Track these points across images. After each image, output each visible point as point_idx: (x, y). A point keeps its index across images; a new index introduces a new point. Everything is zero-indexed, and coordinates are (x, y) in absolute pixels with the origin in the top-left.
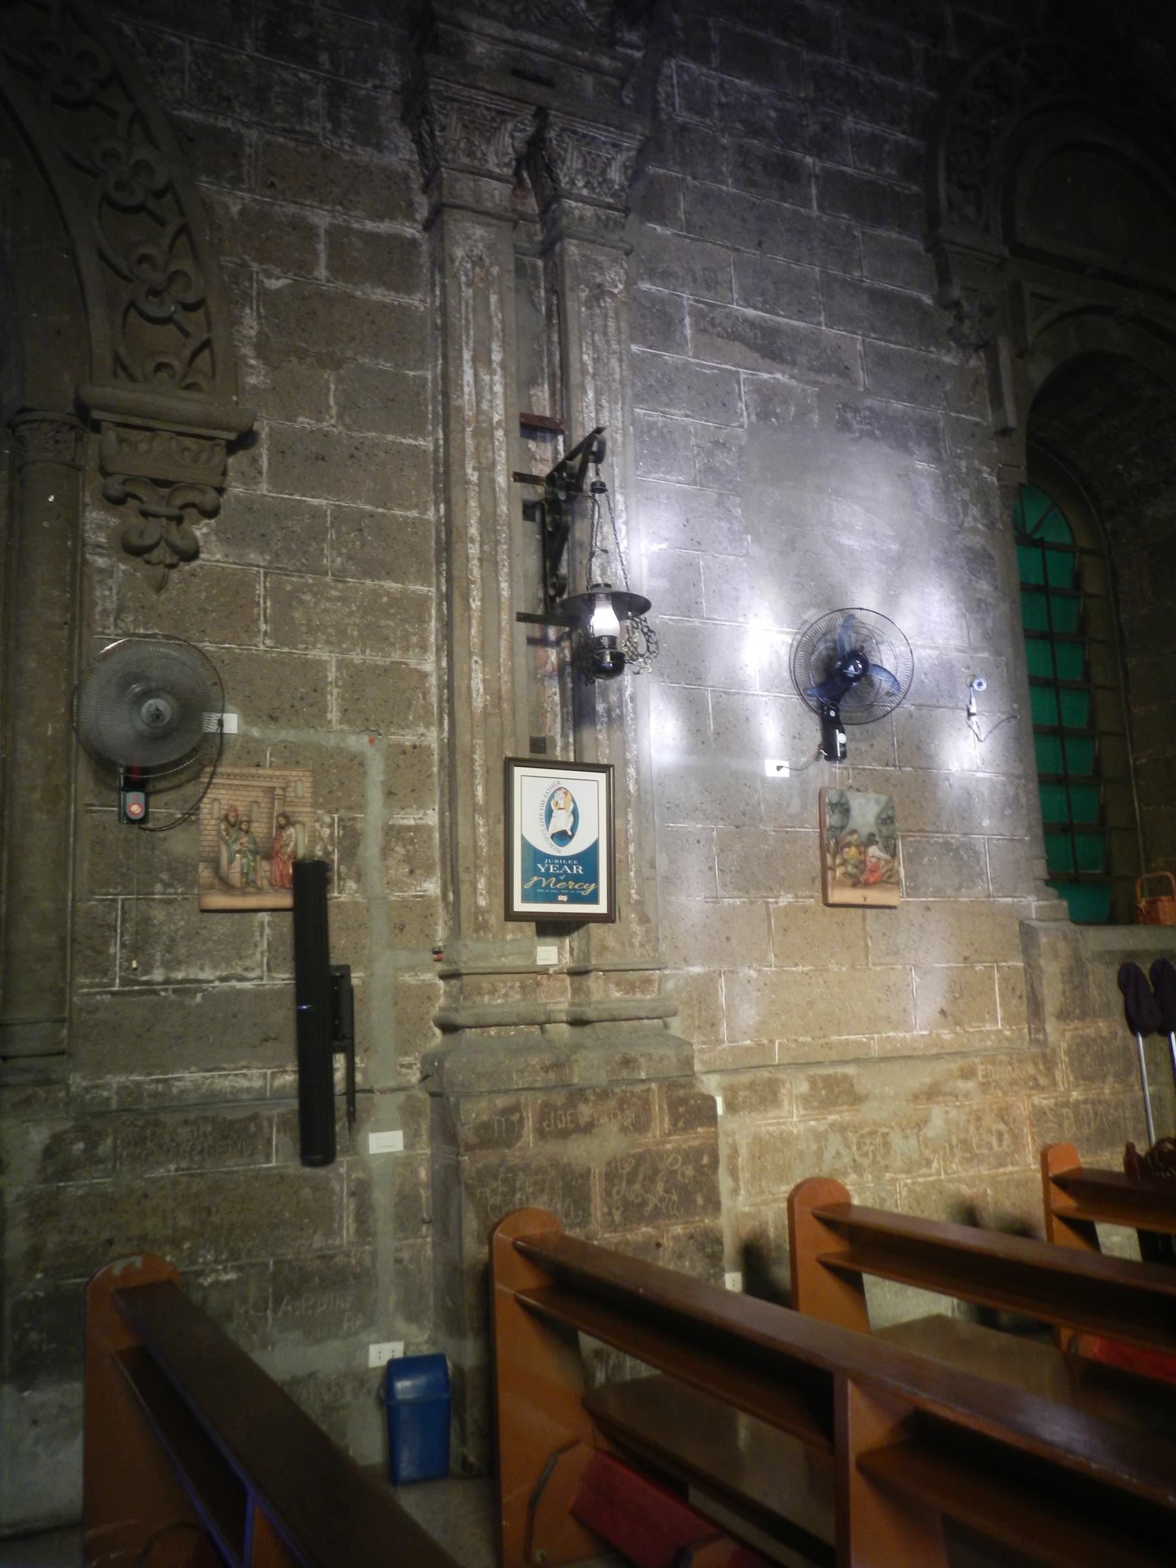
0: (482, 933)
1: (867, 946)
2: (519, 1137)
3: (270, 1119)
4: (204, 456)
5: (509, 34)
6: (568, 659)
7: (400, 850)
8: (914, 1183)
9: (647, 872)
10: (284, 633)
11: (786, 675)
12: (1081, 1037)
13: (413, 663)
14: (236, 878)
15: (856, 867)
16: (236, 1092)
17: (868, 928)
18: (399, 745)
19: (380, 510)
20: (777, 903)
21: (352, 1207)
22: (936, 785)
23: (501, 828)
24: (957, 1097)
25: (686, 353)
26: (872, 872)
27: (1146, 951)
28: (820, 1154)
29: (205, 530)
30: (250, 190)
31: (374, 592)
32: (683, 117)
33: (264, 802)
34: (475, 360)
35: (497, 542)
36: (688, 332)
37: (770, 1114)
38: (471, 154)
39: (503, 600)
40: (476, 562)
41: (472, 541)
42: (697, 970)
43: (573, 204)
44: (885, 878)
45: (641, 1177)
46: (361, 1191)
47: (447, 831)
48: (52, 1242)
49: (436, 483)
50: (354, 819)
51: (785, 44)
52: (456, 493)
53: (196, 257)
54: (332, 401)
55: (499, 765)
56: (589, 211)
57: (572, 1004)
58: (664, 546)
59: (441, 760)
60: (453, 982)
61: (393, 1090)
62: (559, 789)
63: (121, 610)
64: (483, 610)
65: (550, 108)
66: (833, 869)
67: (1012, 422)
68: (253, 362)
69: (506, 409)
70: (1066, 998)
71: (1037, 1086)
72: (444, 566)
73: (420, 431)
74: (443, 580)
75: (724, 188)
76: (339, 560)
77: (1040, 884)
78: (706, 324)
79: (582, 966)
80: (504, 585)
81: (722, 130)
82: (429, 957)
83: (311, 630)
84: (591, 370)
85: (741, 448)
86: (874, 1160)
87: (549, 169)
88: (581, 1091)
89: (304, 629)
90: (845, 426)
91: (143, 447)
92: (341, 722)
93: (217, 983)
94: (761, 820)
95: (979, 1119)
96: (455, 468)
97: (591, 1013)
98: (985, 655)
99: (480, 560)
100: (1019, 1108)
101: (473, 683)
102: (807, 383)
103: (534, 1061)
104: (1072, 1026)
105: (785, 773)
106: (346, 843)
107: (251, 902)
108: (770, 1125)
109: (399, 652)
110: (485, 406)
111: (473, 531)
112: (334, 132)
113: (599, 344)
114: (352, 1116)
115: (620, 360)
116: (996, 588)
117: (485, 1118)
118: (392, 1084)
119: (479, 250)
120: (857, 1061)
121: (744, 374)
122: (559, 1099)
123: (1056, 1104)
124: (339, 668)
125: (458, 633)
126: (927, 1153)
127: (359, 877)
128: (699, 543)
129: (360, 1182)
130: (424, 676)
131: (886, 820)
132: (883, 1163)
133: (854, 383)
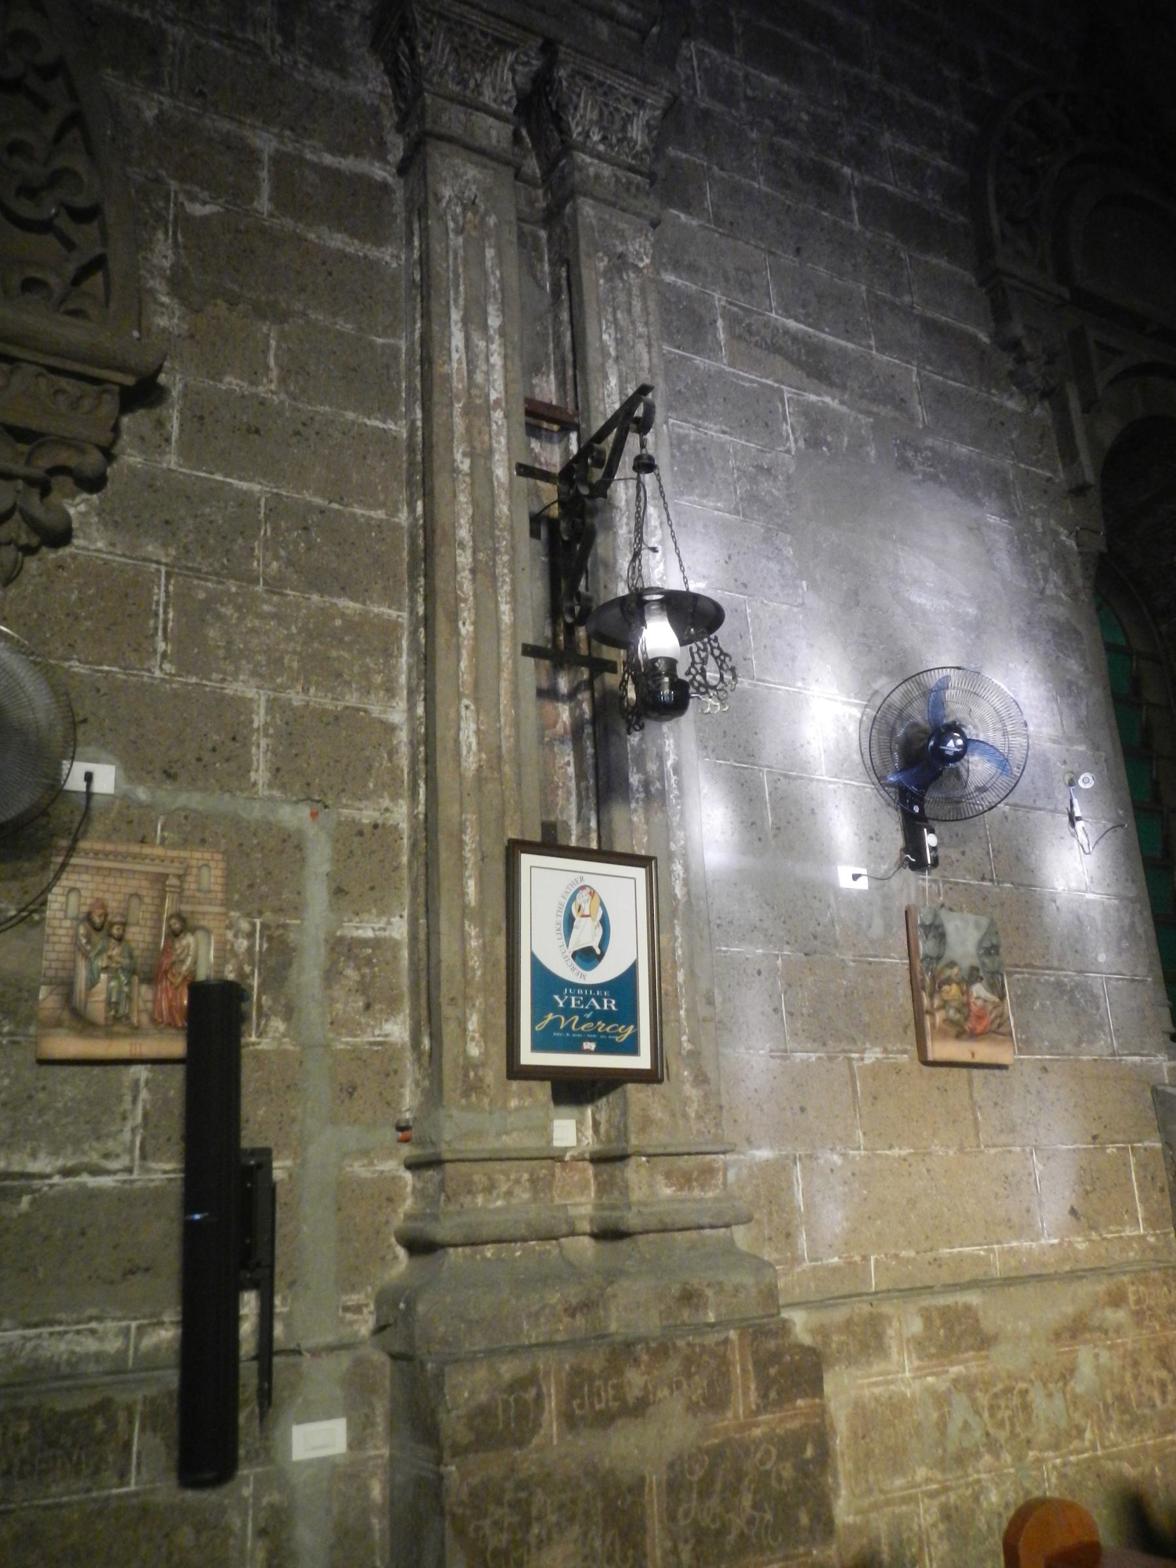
0: (474, 1098)
1: (976, 1119)
2: (537, 1426)
3: (129, 1409)
4: (87, 403)
6: (588, 715)
7: (352, 973)
8: (1064, 1465)
9: (703, 1010)
11: (856, 757)
13: (376, 710)
14: (97, 1008)
15: (958, 1010)
16: (76, 1360)
17: (975, 1095)
19: (335, 506)
20: (862, 1059)
21: (261, 1555)
22: (1041, 908)
23: (501, 941)
24: (1106, 1332)
25: (720, 360)
26: (980, 1018)
28: (942, 1425)
29: (82, 508)
30: (172, 95)
31: (326, 614)
32: (704, 102)
33: (149, 895)
34: (465, 321)
35: (496, 551)
36: (722, 336)
37: (875, 1368)
38: (463, 83)
39: (503, 627)
40: (466, 573)
41: (462, 545)
42: (764, 1154)
43: (588, 160)
44: (995, 1026)
45: (718, 1486)
47: (422, 947)
49: (410, 477)
50: (285, 926)
52: (441, 482)
53: (90, 153)
54: (272, 362)
55: (499, 851)
56: (607, 171)
57: (599, 1207)
59: (414, 847)
60: (429, 1173)
61: (331, 1349)
62: (583, 888)
64: (476, 637)
65: (561, 43)
66: (931, 1013)
67: (1090, 476)
68: (165, 299)
69: (506, 386)
72: (422, 581)
73: (389, 412)
74: (420, 600)
76: (275, 565)
77: (1167, 1038)
78: (740, 330)
79: (616, 1148)
80: (505, 608)
81: (752, 125)
82: (391, 1135)
84: (613, 353)
85: (789, 478)
86: (1012, 1432)
87: (557, 119)
88: (628, 1345)
89: (221, 653)
90: (905, 465)
92: (270, 786)
93: (56, 1179)
94: (836, 945)
95: (1136, 1364)
96: (440, 450)
97: (632, 1220)
98: (1082, 748)
99: (473, 571)
101: (462, 737)
102: (860, 411)
103: (554, 1298)
105: (863, 884)
106: (272, 962)
107: (121, 1048)
108: (876, 1384)
109: (356, 695)
110: (479, 378)
111: (464, 533)
112: (285, 46)
113: (622, 323)
114: (265, 1396)
115: (649, 346)
116: (1086, 669)
117: (483, 1398)
118: (330, 1339)
120: (974, 1284)
121: (787, 392)
122: (597, 1365)
124: (270, 710)
125: (442, 665)
126: (1077, 1416)
127: (289, 1013)
128: (745, 586)
129: (275, 1510)
130: (391, 729)
131: (990, 950)
132: (1023, 1436)
133: (912, 419)
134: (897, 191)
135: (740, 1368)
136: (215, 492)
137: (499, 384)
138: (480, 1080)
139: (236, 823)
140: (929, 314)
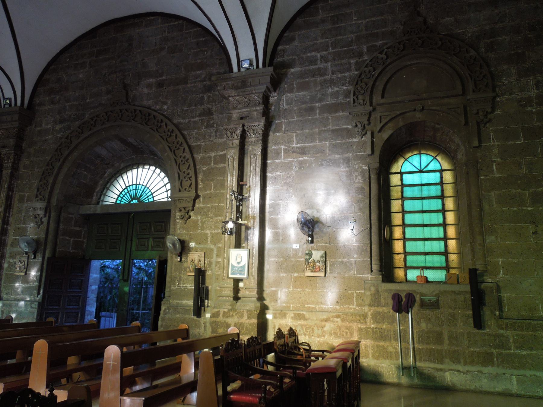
5: (239, 111)
8: (320, 340)
12: (376, 311)
26: (317, 269)
27: (404, 290)
30: (202, 154)
31: (217, 220)
32: (286, 107)
36: (282, 154)
42: (274, 289)
46: (205, 323)
48: (164, 324)
51: (314, 79)
58: (273, 201)
63: (180, 228)
70: (372, 301)
78: (287, 151)
83: (206, 228)
85: (293, 177)
86: (309, 333)
90: (322, 165)
95: (340, 328)
102: (312, 157)
104: (374, 308)
105: (298, 247)
110: (231, 184)
112: (216, 138)
119: (232, 154)
121: (295, 160)
123: (366, 327)
135: (245, 314)
136: (205, 207)
137: (234, 183)
138: (224, 278)
139: (206, 248)
140: (334, 128)
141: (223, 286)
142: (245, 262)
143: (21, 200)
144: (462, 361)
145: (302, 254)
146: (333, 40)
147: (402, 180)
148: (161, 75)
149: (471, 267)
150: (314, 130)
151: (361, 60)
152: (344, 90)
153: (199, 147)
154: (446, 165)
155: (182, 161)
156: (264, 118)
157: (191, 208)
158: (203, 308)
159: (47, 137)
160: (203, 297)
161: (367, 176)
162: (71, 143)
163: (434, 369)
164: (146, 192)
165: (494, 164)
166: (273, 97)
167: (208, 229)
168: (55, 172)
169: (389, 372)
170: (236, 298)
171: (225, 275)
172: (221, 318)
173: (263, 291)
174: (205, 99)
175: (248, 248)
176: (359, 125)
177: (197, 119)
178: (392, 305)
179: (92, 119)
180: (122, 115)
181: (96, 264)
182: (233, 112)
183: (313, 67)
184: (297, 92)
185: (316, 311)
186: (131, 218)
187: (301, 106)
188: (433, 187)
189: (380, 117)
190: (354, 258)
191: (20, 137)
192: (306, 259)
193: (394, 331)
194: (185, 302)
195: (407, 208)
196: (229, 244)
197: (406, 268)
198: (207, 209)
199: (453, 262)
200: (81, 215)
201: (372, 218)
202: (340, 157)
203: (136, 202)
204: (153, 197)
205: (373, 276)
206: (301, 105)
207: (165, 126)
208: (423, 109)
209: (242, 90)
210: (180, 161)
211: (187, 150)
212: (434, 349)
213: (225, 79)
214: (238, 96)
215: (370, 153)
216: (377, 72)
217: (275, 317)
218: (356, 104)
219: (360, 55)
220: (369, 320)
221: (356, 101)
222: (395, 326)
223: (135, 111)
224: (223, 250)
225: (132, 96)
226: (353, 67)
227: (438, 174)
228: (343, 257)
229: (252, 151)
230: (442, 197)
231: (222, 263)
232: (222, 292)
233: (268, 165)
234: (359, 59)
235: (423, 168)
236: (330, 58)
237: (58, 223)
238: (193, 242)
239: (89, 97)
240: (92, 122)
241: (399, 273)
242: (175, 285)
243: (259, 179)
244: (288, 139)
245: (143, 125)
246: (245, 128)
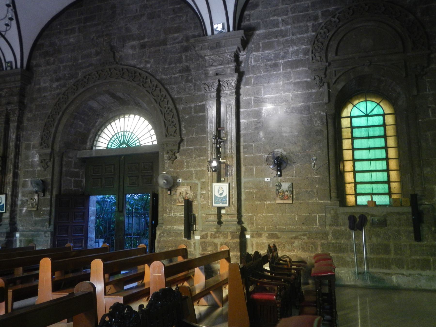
1: (286, 210)
2: (208, 238)
5: (215, 68)
7: (203, 197)
10: (188, 167)
14: (181, 201)
15: (281, 196)
18: (203, 181)
21: (193, 245)
26: (285, 197)
27: (358, 213)
30: (184, 104)
31: (199, 159)
32: (253, 64)
36: (253, 104)
37: (260, 239)
38: (209, 90)
42: (250, 214)
43: (226, 92)
46: (194, 243)
48: (160, 245)
51: (277, 39)
63: (168, 167)
68: (184, 129)
70: (332, 222)
71: (323, 239)
75: (261, 74)
91: (169, 145)
100: (317, 243)
102: (278, 106)
104: (333, 227)
105: (269, 180)
106: (195, 196)
110: (211, 129)
112: (195, 91)
123: (328, 243)
134: (292, 59)
135: (229, 235)
136: (189, 149)
140: (296, 81)
141: (209, 213)
142: (226, 193)
143: (28, 147)
144: (405, 267)
145: (273, 186)
146: (292, 5)
147: (351, 123)
148: (143, 38)
149: (413, 193)
150: (279, 83)
151: (316, 23)
152: (303, 49)
153: (181, 99)
154: (388, 110)
155: (166, 111)
156: (237, 74)
157: (177, 151)
158: (192, 232)
159: (46, 94)
160: (192, 223)
161: (325, 121)
162: (68, 98)
163: (383, 273)
164: (133, 138)
165: (430, 109)
166: (243, 55)
167: (192, 167)
168: (56, 124)
169: (347, 277)
170: (220, 223)
171: (209, 204)
172: (209, 239)
173: (242, 216)
174: (183, 58)
175: (228, 182)
176: (317, 79)
177: (177, 75)
178: (348, 224)
179: (85, 77)
180: (111, 74)
181: (93, 199)
182: (209, 69)
183: (276, 29)
184: (263, 50)
185: (286, 231)
186: (122, 159)
187: (267, 63)
188: (377, 128)
189: (335, 71)
190: (316, 188)
191: (22, 94)
192: (277, 190)
193: (350, 245)
194: (176, 227)
195: (356, 146)
196: (212, 179)
197: (356, 195)
198: (191, 150)
199: (395, 189)
200: (79, 158)
201: (330, 155)
202: (301, 105)
203: (125, 147)
204: (139, 142)
205: (332, 202)
206: (267, 62)
207: (150, 82)
208: (370, 64)
209: (217, 50)
210: (165, 112)
211: (170, 101)
212: (383, 258)
213: (202, 41)
214: (213, 55)
215: (327, 101)
216: (331, 33)
217: (252, 237)
218: (314, 61)
219: (316, 18)
220: (330, 237)
221: (314, 58)
222: (351, 241)
223: (122, 69)
224: (207, 184)
225: (118, 57)
226: (310, 29)
227: (381, 118)
228: (307, 187)
229: (228, 102)
230: (385, 136)
231: (206, 195)
232: (208, 218)
233: (241, 113)
234: (315, 22)
235: (368, 112)
236: (290, 21)
237: (61, 166)
238: (180, 178)
239: (80, 59)
240: (86, 80)
241: (351, 199)
242: (167, 214)
243: (235, 125)
244: (256, 91)
245: (131, 82)
246: (221, 83)
